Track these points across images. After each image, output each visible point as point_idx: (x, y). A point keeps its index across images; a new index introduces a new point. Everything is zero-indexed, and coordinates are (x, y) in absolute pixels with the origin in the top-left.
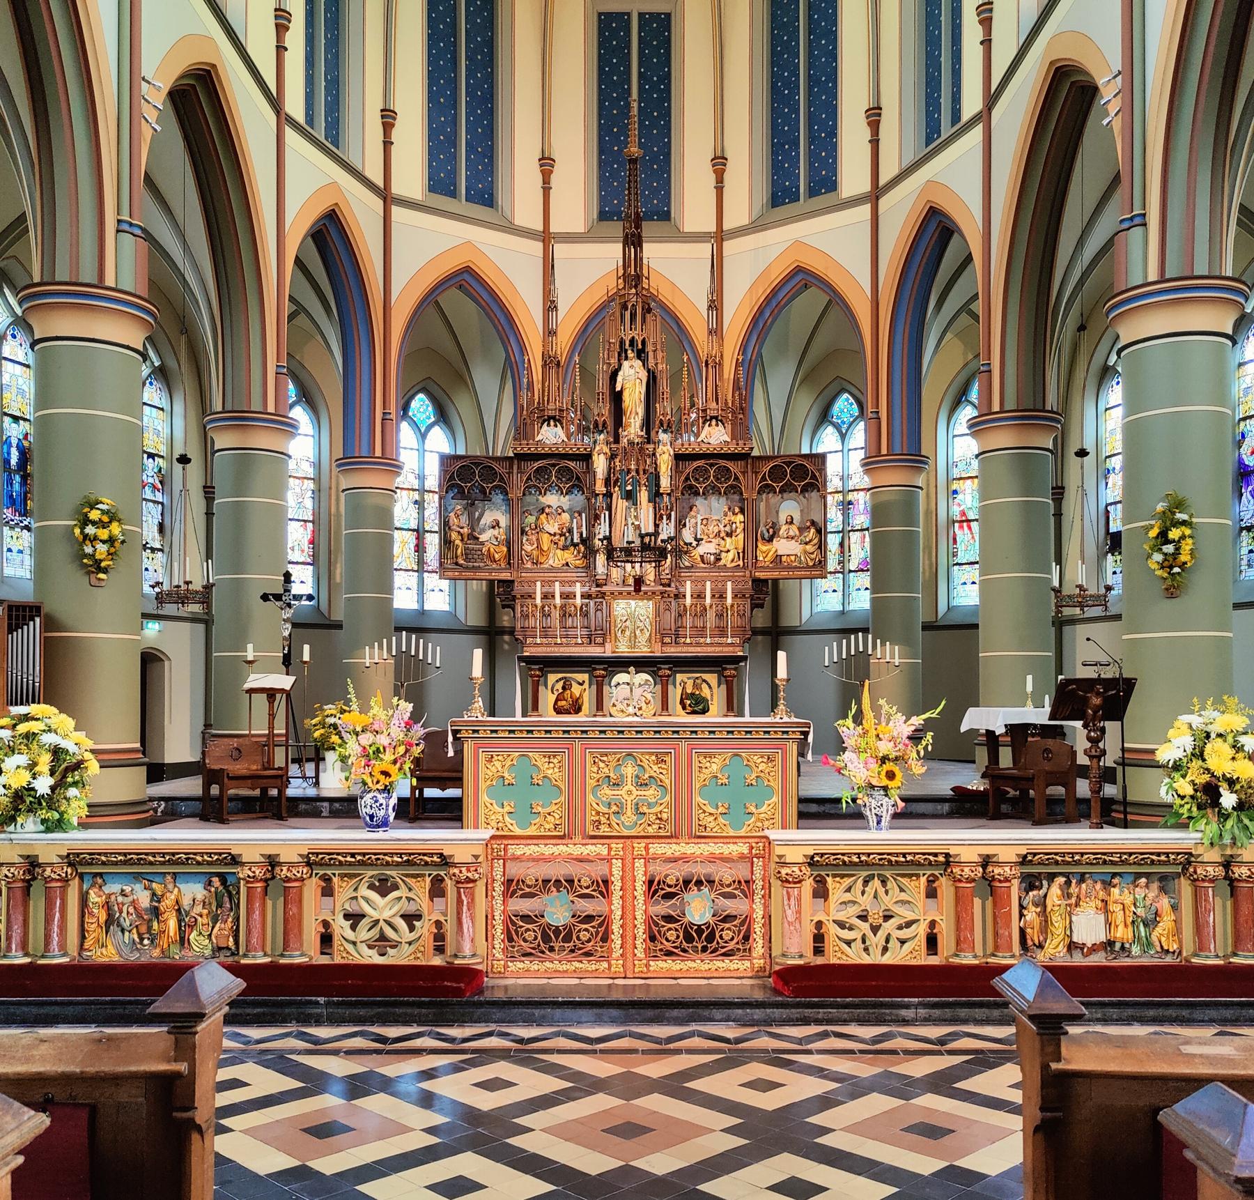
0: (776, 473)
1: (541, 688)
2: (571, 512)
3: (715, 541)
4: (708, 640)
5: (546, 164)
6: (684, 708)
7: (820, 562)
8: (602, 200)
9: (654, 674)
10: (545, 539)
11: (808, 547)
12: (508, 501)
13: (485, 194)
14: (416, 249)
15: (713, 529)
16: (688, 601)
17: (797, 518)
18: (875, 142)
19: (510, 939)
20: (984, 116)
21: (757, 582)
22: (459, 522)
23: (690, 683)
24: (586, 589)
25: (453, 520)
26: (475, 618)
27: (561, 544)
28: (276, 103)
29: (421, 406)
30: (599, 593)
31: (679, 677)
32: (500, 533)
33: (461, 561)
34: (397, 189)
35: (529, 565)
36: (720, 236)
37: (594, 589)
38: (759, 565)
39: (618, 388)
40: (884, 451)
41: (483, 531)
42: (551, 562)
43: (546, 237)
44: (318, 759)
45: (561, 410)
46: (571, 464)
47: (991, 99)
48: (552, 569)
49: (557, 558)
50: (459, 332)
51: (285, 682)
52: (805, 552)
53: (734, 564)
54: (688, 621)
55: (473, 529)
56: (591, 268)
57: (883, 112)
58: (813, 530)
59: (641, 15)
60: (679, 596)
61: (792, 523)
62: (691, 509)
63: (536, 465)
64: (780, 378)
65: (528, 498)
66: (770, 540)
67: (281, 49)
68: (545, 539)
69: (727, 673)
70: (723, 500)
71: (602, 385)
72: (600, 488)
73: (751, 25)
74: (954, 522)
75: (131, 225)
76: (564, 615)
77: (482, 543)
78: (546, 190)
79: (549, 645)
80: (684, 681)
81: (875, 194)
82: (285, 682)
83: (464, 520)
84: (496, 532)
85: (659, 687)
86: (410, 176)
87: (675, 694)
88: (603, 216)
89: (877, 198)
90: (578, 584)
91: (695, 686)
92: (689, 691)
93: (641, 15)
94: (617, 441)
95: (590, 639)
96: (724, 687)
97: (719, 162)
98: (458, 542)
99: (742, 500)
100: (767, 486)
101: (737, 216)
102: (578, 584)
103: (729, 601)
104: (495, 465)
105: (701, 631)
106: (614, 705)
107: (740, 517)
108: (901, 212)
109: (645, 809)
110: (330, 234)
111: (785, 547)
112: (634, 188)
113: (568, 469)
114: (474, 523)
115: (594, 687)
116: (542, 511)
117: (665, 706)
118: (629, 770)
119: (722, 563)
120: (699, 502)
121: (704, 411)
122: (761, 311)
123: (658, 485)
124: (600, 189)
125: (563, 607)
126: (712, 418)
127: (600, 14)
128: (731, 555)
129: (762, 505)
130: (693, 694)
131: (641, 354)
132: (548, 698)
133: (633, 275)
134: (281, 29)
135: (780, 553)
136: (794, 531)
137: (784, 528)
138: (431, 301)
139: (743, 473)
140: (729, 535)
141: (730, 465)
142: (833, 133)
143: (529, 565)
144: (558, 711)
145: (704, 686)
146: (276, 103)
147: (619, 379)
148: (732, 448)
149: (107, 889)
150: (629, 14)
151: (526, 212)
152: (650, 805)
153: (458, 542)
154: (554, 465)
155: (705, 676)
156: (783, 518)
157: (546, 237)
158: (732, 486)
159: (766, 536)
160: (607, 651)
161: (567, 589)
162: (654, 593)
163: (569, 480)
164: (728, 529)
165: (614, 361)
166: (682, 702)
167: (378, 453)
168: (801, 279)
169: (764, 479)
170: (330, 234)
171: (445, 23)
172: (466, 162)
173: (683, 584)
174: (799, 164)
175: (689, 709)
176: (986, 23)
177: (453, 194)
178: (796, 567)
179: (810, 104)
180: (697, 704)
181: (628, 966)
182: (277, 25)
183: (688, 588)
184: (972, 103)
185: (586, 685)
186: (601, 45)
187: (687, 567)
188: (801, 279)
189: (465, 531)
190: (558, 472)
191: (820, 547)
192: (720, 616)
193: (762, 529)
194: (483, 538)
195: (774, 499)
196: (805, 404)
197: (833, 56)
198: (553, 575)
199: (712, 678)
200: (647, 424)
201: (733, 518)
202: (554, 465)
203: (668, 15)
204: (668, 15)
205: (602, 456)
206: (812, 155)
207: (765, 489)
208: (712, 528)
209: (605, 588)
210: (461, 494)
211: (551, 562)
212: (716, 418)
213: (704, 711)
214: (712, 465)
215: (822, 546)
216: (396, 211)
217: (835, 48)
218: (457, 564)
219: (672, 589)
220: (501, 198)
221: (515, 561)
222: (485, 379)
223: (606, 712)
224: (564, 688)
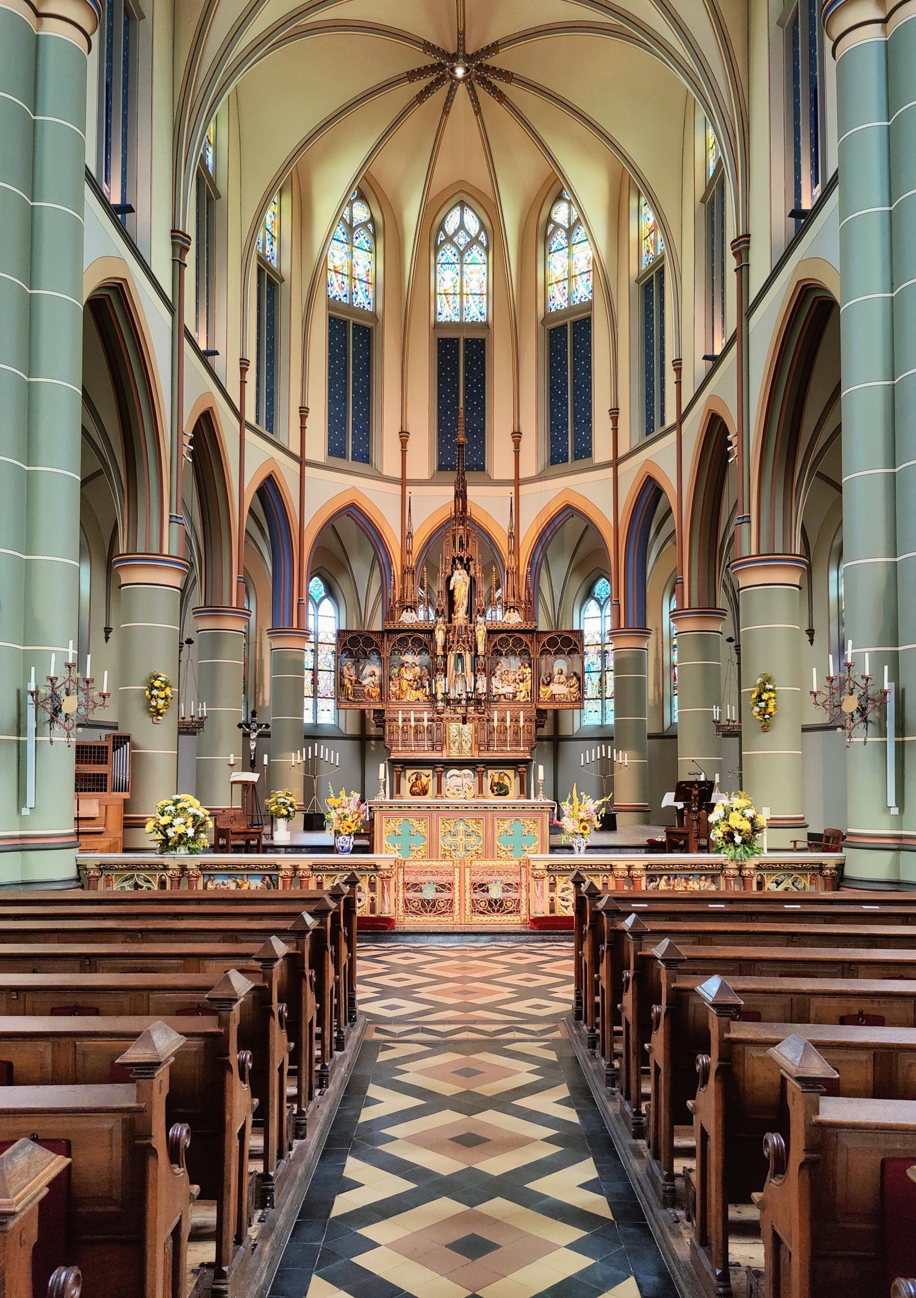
0: (552, 642)
1: (402, 779)
2: (421, 666)
3: (513, 685)
4: (509, 749)
5: (404, 436)
6: (493, 792)
8: (440, 458)
9: (474, 770)
10: (405, 684)
11: (572, 689)
12: (381, 659)
13: (364, 456)
14: (321, 493)
15: (511, 677)
16: (496, 723)
17: (565, 670)
18: (615, 430)
19: (406, 906)
20: (678, 426)
21: (539, 711)
22: (349, 672)
24: (431, 715)
25: (346, 672)
26: (352, 729)
27: (414, 686)
28: (240, 415)
29: (316, 587)
30: (438, 720)
31: (490, 772)
32: (376, 680)
33: (351, 698)
34: (308, 456)
36: (517, 482)
37: (436, 716)
39: (451, 588)
40: (622, 626)
41: (365, 678)
43: (403, 482)
44: (272, 823)
45: (415, 602)
46: (421, 636)
47: (682, 417)
48: (409, 703)
49: (412, 695)
50: (347, 542)
51: (253, 777)
52: (570, 692)
54: (495, 736)
55: (358, 678)
56: (434, 503)
57: (620, 411)
58: (575, 679)
59: (466, 340)
61: (561, 674)
63: (399, 636)
64: (560, 567)
65: (393, 657)
66: (548, 684)
67: (243, 382)
68: (405, 684)
69: (520, 770)
70: (518, 659)
71: (440, 586)
72: (440, 652)
73: (537, 351)
74: (675, 666)
75: (177, 517)
76: (417, 732)
77: (364, 686)
78: (404, 452)
79: (406, 751)
80: (493, 774)
81: (616, 462)
82: (253, 777)
83: (353, 671)
84: (373, 679)
85: (477, 778)
86: (317, 449)
87: (487, 783)
88: (441, 468)
89: (617, 465)
90: (426, 713)
93: (466, 340)
94: (450, 621)
95: (433, 748)
96: (518, 778)
97: (517, 436)
98: (349, 685)
99: (530, 659)
100: (546, 650)
101: (528, 469)
102: (426, 713)
103: (522, 724)
104: (372, 636)
105: (504, 743)
107: (529, 670)
108: (631, 474)
109: (469, 848)
110: (269, 491)
111: (557, 689)
112: (461, 450)
113: (420, 639)
114: (359, 673)
115: (436, 778)
116: (403, 665)
117: (481, 790)
118: (461, 827)
119: (517, 699)
120: (503, 660)
121: (506, 603)
122: (544, 531)
123: (476, 650)
124: (439, 450)
125: (416, 727)
126: (511, 607)
127: (439, 339)
128: (523, 694)
129: (543, 662)
130: (498, 783)
131: (467, 568)
132: (406, 786)
133: (461, 512)
134: (243, 371)
136: (563, 679)
137: (557, 677)
138: (330, 526)
139: (531, 642)
141: (522, 637)
142: (589, 420)
143: (394, 700)
145: (506, 777)
146: (240, 415)
147: (452, 582)
148: (524, 626)
149: (215, 882)
150: (458, 339)
151: (391, 468)
152: (472, 846)
153: (349, 685)
154: (410, 636)
155: (506, 772)
156: (556, 670)
157: (403, 482)
158: (524, 650)
160: (444, 756)
161: (418, 715)
163: (420, 646)
164: (521, 677)
165: (449, 571)
167: (295, 626)
168: (568, 512)
169: (544, 646)
170: (269, 491)
171: (339, 348)
172: (353, 436)
173: (492, 712)
174: (568, 440)
175: (496, 793)
176: (678, 371)
177: (343, 456)
179: (574, 401)
180: (501, 789)
181: (462, 916)
182: (241, 368)
183: (496, 715)
184: (671, 418)
185: (431, 777)
186: (439, 359)
188: (568, 512)
189: (353, 678)
190: (413, 640)
192: (516, 733)
193: (543, 677)
194: (365, 682)
195: (550, 658)
196: (576, 585)
197: (589, 372)
198: (409, 708)
199: (511, 773)
200: (469, 611)
201: (524, 670)
202: (410, 636)
203: (483, 340)
204: (483, 340)
205: (441, 632)
206: (575, 433)
207: (545, 652)
208: (511, 679)
209: (442, 716)
210: (351, 655)
212: (513, 607)
213: (506, 794)
214: (511, 637)
215: (581, 688)
216: (308, 470)
217: (590, 367)
218: (348, 699)
219: (486, 715)
220: (375, 457)
222: (360, 567)
223: (443, 794)
224: (416, 779)
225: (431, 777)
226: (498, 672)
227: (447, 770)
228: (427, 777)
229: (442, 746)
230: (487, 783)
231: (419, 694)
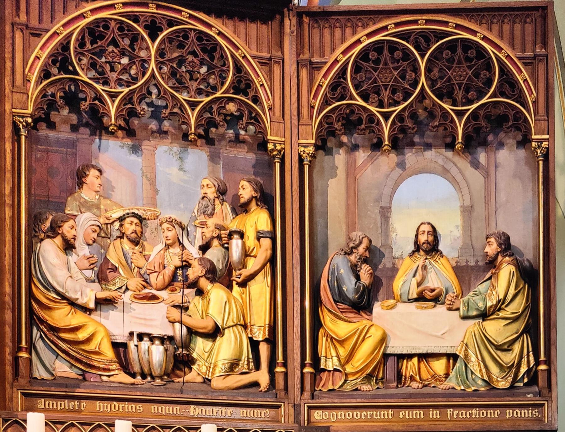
7: (533, 377)
11: (496, 329)
38: (327, 383)
53: (236, 380)
58: (506, 271)
62: (80, 178)
66: (362, 304)
70: (198, 157)
107: (259, 219)
119: (193, 376)
120: (112, 153)
128: (227, 347)
129: (335, 191)
135: (396, 346)
136: (440, 276)
140: (223, 276)
156: (403, 233)
159: (349, 286)
164: (215, 254)
178: (451, 394)
187: (65, 382)
191: (531, 329)
226: (82, 225)
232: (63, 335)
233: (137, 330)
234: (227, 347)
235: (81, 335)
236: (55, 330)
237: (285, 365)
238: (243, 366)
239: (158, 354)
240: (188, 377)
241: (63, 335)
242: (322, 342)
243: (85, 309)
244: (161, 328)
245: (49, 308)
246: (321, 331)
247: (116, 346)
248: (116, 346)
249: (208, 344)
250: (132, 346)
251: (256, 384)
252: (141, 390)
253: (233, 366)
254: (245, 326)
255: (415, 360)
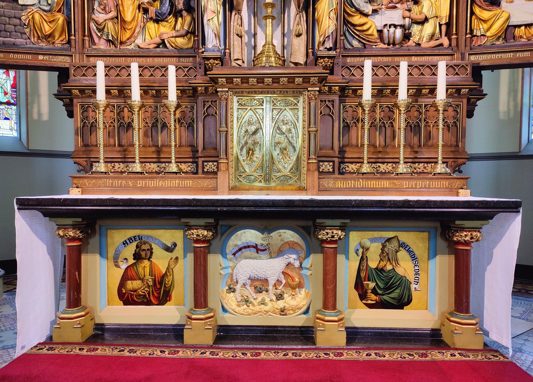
6: (363, 296)
23: (375, 249)
31: (355, 238)
35: (102, 45)
42: (139, 41)
53: (433, 43)
54: (363, 135)
60: (349, 91)
80: (364, 244)
87: (347, 269)
91: (384, 254)
92: (373, 264)
106: (232, 290)
115: (191, 257)
117: (329, 300)
130: (380, 270)
135: (514, 21)
143: (102, 45)
144: (127, 298)
145: (402, 254)
155: (404, 237)
162: (306, 79)
166: (359, 285)
187: (358, 49)
199: (416, 239)
211: (139, 41)
213: (402, 303)
221: (77, 38)
224: (137, 257)
225: (179, 251)
227: (231, 230)
228: (170, 251)
229: (215, 158)
230: (347, 269)
231: (165, 30)
232: (357, 28)
233: (389, 23)
234: (429, 28)
235: (365, 28)
236: (354, 25)
237: (456, 34)
238: (435, 37)
239: (399, 33)
240: (409, 44)
241: (357, 28)
242: (475, 22)
243: (366, 15)
244: (398, 21)
245: (352, 16)
246: (474, 17)
247: (378, 31)
248: (378, 31)
249: (420, 27)
250: (385, 30)
251: (441, 45)
252: (391, 50)
253: (432, 37)
254: (437, 17)
255: (523, 28)
